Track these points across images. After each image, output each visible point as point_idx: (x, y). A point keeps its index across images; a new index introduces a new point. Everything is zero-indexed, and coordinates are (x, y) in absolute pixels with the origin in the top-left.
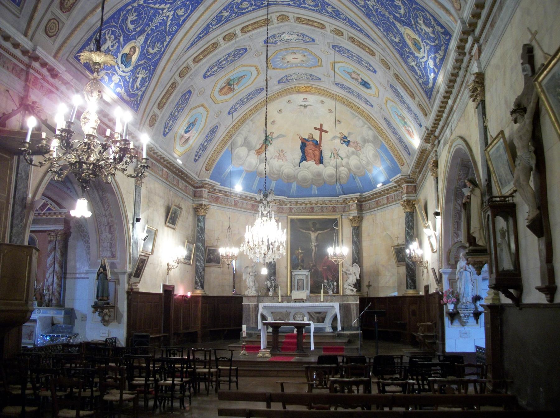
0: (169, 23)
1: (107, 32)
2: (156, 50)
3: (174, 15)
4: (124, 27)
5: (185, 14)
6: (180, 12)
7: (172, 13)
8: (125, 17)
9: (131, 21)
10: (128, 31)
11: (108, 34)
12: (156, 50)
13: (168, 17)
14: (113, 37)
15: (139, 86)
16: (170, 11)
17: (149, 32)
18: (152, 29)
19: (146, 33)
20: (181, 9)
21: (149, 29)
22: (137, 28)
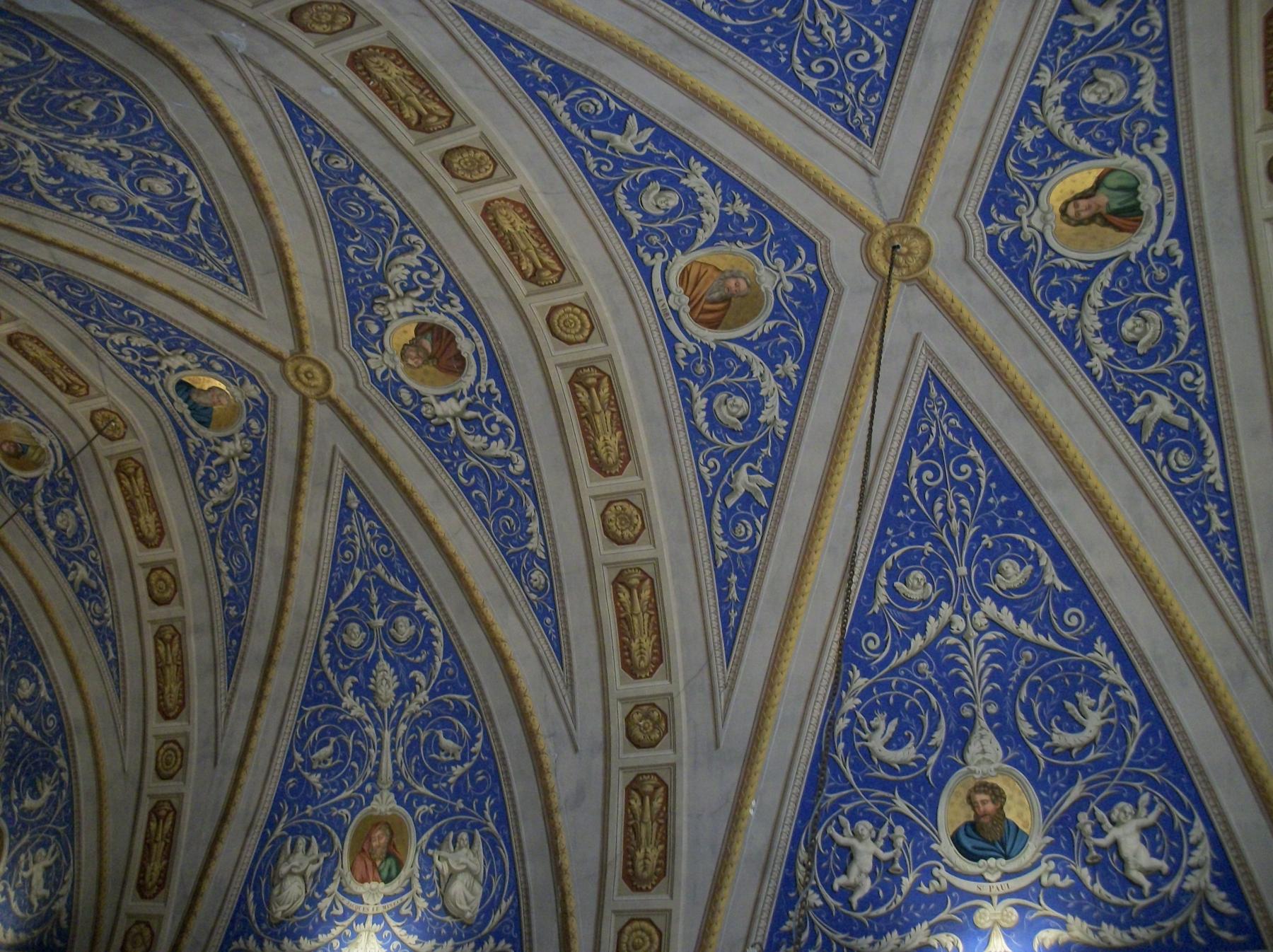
0: (28, 727)
1: (832, 831)
2: (47, 792)
3: (18, 706)
4: (882, 774)
5: (37, 681)
6: (26, 688)
7: (13, 708)
8: (854, 753)
9: (888, 745)
10: (905, 768)
11: (840, 829)
12: (47, 792)
13: (15, 723)
14: (865, 827)
15: (47, 893)
16: (7, 709)
17: (993, 709)
18: (993, 696)
19: (982, 722)
20: (19, 685)
21: (979, 708)
22: (930, 738)
